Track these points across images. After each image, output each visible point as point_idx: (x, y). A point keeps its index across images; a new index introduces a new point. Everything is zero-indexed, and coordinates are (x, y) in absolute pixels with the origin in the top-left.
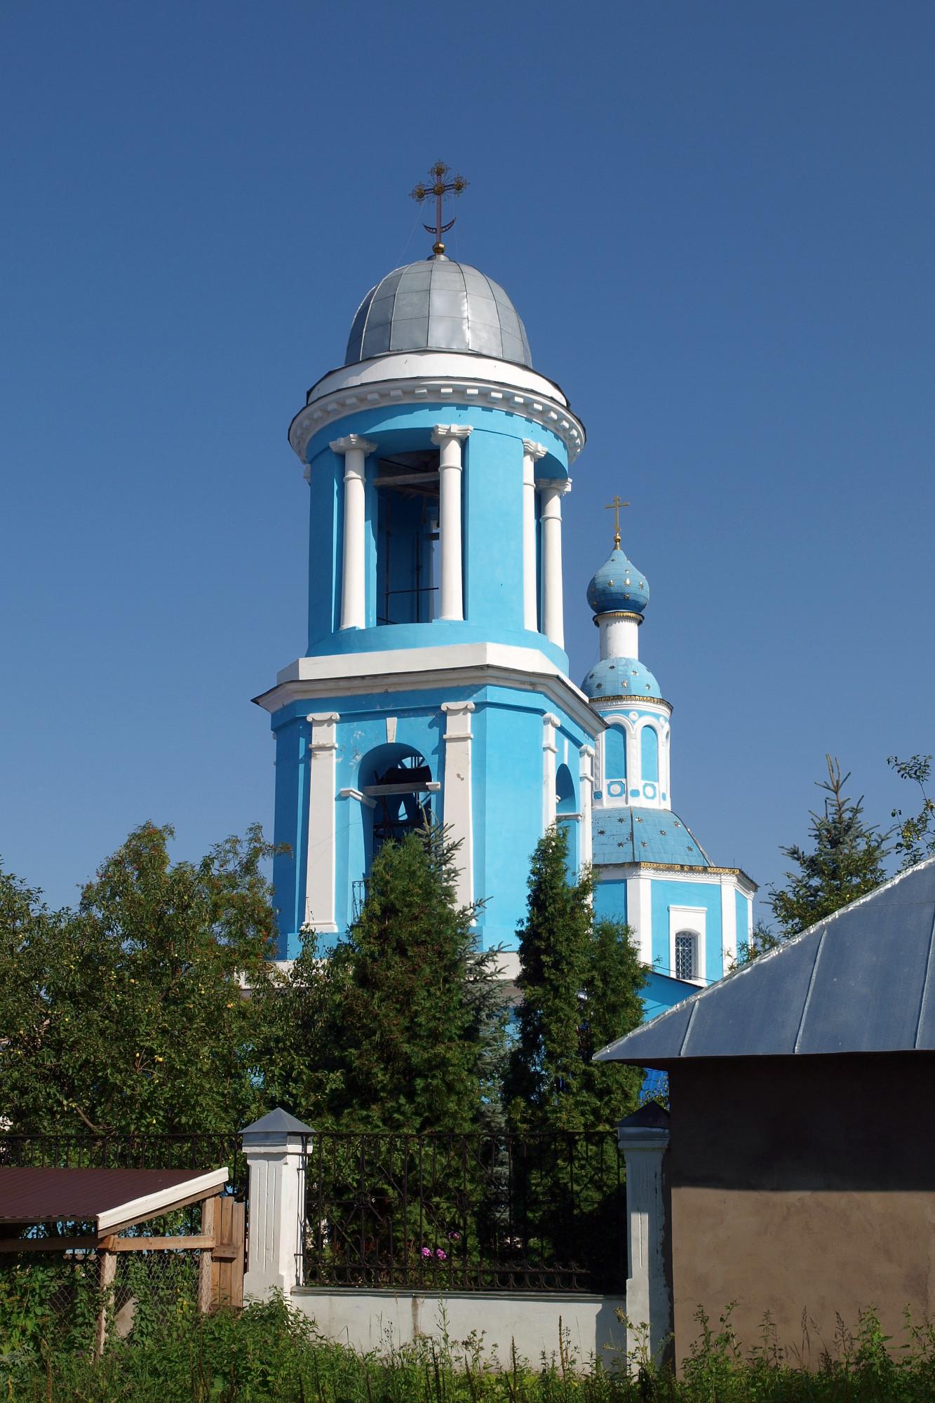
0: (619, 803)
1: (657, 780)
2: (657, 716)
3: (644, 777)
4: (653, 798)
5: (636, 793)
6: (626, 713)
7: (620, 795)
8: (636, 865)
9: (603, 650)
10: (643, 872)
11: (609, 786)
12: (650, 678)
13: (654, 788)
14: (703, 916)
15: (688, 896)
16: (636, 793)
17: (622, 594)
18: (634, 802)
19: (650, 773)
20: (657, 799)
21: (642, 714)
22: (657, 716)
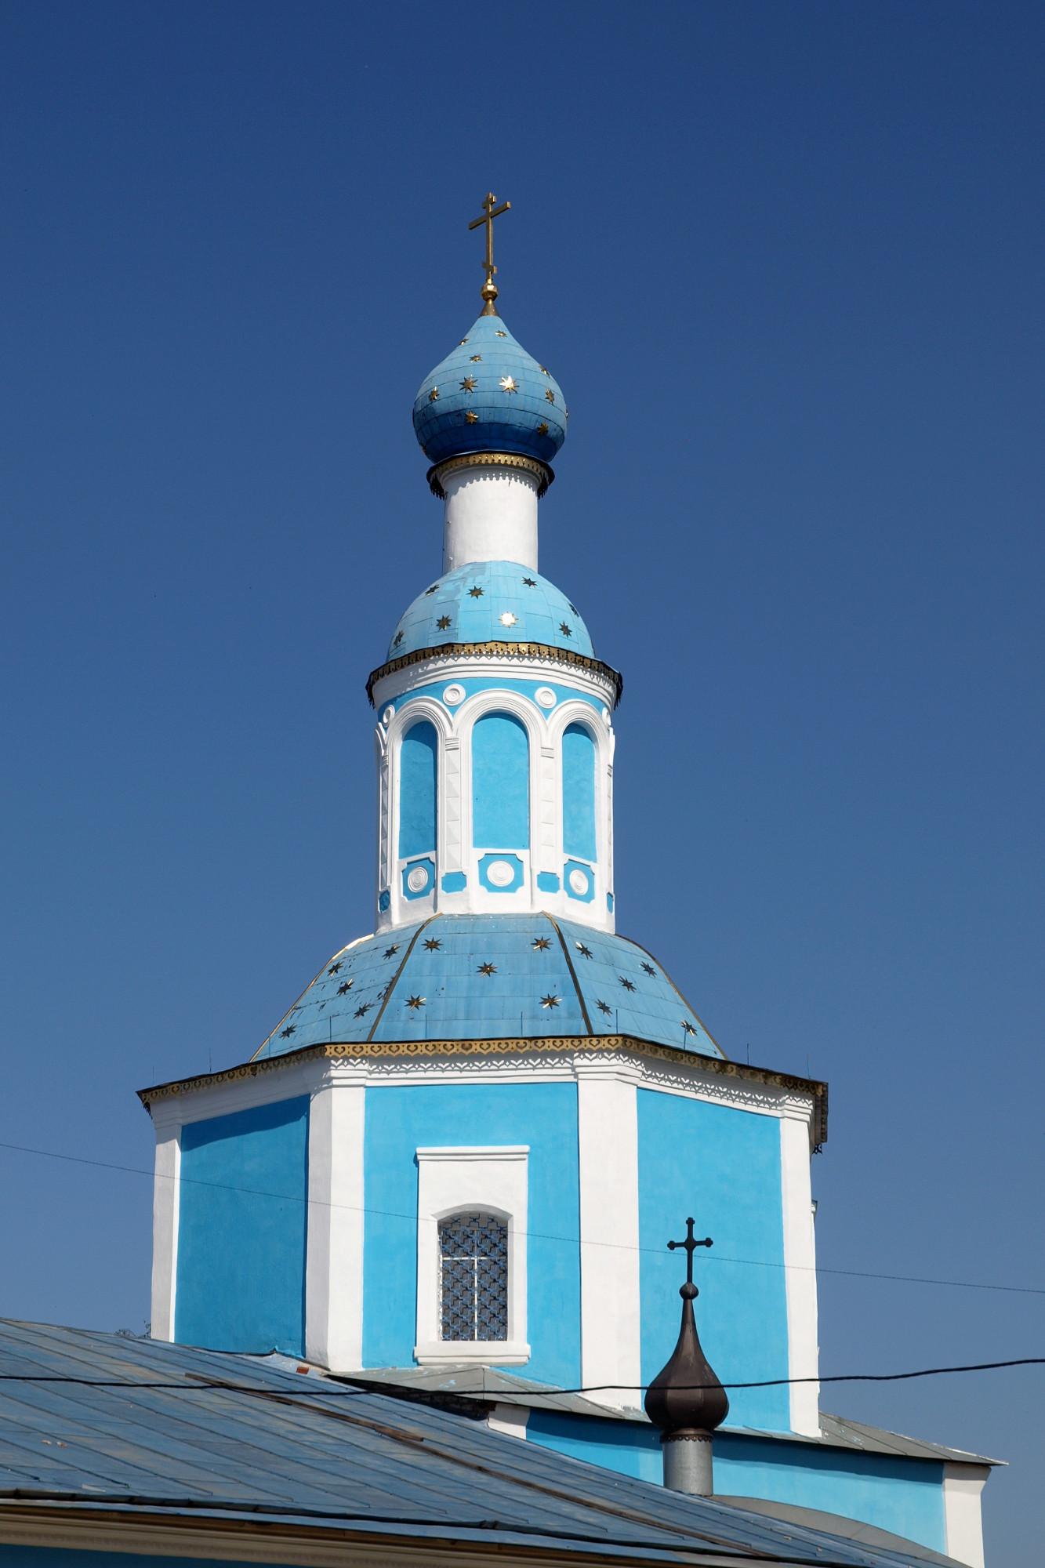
0: (422, 912)
1: (527, 845)
2: (527, 688)
3: (477, 843)
4: (512, 888)
5: (457, 881)
6: (437, 689)
7: (424, 893)
8: (315, 1053)
9: (432, 554)
10: (339, 1072)
11: (405, 873)
12: (552, 605)
13: (517, 863)
14: (522, 1168)
15: (469, 1123)
16: (457, 881)
17: (460, 413)
18: (450, 905)
19: (577, 839)
20: (523, 891)
21: (474, 686)
22: (527, 688)
